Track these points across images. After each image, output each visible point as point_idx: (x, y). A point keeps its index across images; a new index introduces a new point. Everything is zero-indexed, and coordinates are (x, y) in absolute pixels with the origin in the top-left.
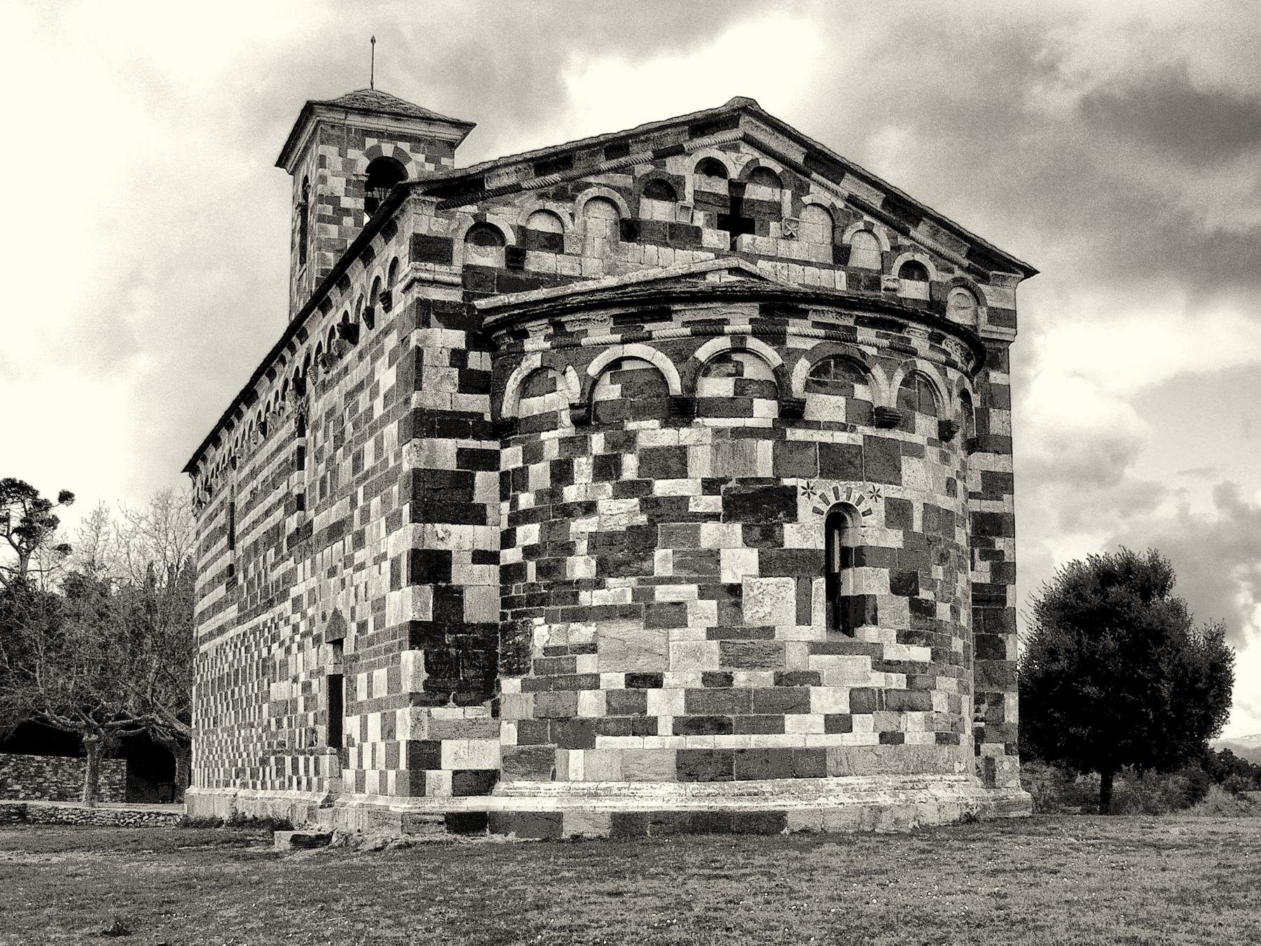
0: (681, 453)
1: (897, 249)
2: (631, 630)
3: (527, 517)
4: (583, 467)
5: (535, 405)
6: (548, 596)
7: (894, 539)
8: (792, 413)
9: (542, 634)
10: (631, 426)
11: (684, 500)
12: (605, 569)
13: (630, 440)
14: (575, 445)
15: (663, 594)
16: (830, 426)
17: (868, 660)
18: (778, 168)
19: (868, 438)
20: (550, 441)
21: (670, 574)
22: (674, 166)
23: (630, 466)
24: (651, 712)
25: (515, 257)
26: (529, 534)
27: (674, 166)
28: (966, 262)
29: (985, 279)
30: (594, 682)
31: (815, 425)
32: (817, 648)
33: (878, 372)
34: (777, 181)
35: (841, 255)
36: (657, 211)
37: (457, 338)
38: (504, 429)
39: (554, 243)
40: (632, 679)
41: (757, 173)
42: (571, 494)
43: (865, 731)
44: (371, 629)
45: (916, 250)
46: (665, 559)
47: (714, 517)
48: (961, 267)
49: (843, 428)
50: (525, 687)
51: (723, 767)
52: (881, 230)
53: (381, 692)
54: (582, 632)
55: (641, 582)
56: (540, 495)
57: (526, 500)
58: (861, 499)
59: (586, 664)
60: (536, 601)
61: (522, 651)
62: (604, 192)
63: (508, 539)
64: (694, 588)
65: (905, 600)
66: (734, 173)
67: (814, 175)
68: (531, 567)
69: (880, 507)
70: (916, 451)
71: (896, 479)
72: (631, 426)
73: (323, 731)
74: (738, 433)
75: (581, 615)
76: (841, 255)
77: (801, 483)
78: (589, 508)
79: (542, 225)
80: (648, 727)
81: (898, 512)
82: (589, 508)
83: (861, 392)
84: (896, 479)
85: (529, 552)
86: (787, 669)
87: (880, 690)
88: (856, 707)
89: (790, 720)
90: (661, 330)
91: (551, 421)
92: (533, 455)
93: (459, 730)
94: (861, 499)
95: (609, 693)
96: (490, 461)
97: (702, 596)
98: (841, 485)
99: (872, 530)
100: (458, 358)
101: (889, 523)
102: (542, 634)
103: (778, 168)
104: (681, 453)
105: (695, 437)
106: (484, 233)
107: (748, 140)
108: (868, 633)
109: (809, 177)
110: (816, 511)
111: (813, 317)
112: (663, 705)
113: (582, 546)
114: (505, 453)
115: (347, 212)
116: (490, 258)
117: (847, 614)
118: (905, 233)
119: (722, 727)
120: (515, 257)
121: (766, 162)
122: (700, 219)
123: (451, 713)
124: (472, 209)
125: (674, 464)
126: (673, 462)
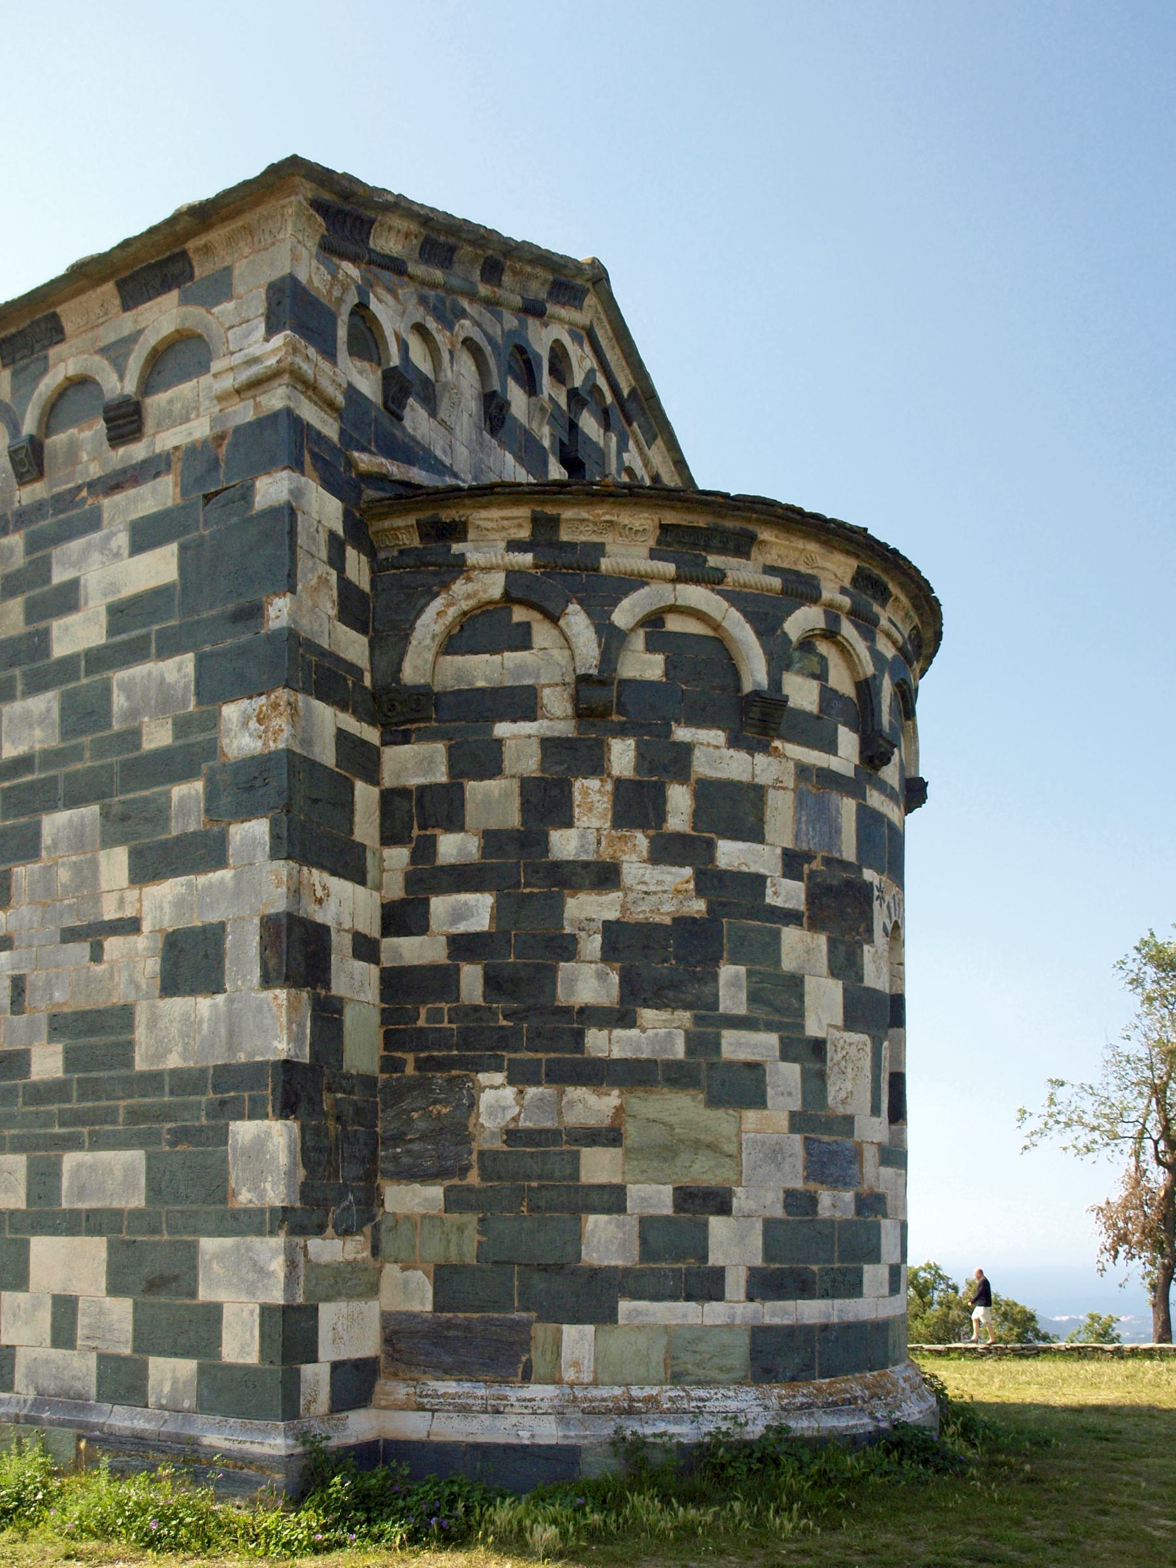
2: (682, 1108)
3: (463, 878)
4: (592, 797)
5: (483, 669)
6: (516, 1032)
10: (682, 734)
11: (758, 882)
13: (678, 761)
14: (574, 755)
15: (737, 1046)
21: (742, 1010)
23: (680, 802)
26: (477, 911)
30: (612, 1199)
40: (686, 1198)
42: (565, 844)
46: (734, 983)
47: (791, 917)
50: (454, 1201)
54: (592, 1105)
55: (698, 1020)
56: (492, 839)
57: (452, 847)
59: (598, 1166)
60: (480, 1044)
61: (458, 1132)
68: (471, 978)
72: (682, 734)
75: (597, 1074)
78: (605, 876)
80: (709, 1286)
85: (464, 946)
90: (743, 572)
91: (522, 702)
92: (485, 760)
95: (647, 1223)
97: (785, 1057)
102: (498, 1102)
104: (755, 793)
105: (772, 769)
112: (733, 1244)
113: (593, 945)
119: (804, 1288)
123: (328, 1249)
126: (732, 808)
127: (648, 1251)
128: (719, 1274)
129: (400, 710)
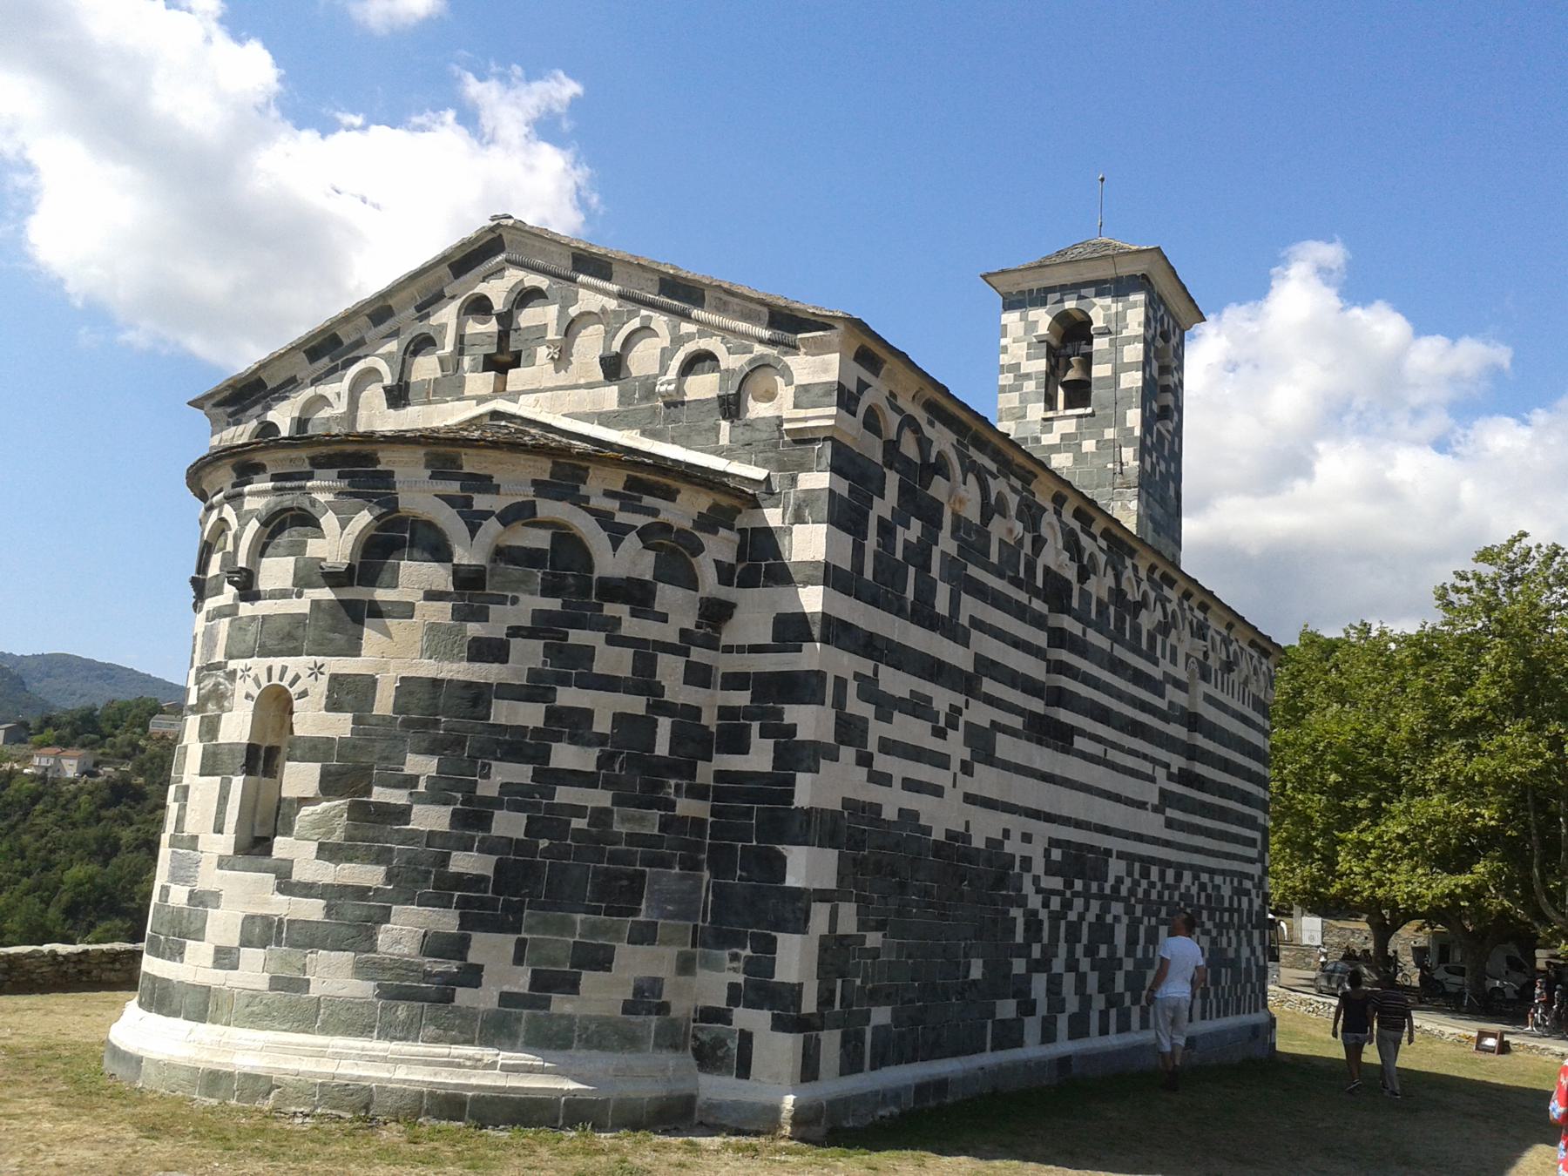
1: (678, 340)
7: (341, 725)
18: (542, 282)
19: (316, 604)
28: (767, 334)
32: (223, 863)
33: (329, 521)
35: (613, 367)
41: (527, 297)
43: (254, 970)
45: (701, 334)
48: (761, 341)
52: (660, 321)
58: (297, 678)
65: (341, 803)
66: (498, 305)
67: (582, 278)
71: (354, 650)
81: (349, 694)
84: (354, 650)
87: (281, 921)
94: (297, 678)
98: (277, 662)
101: (333, 706)
103: (542, 282)
109: (574, 280)
110: (248, 696)
111: (271, 470)
115: (1028, 376)
118: (687, 317)
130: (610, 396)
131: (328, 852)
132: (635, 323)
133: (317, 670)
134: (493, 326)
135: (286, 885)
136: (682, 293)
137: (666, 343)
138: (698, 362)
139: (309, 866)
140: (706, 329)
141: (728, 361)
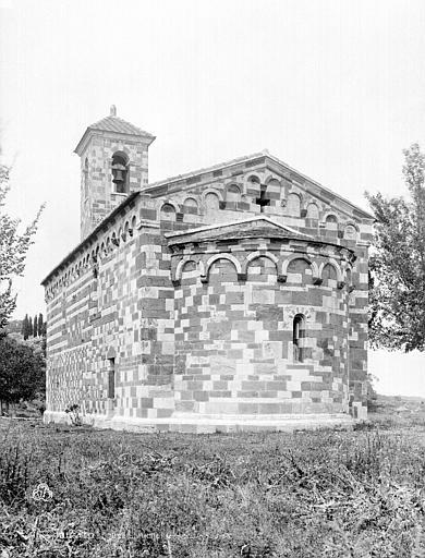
0: (242, 296)
2: (224, 360)
4: (205, 299)
5: (186, 275)
8: (282, 280)
9: (191, 360)
10: (223, 284)
11: (242, 312)
12: (214, 336)
15: (234, 346)
16: (295, 285)
17: (307, 371)
20: (194, 289)
21: (236, 339)
22: (239, 180)
23: (223, 299)
24: (229, 389)
25: (180, 217)
26: (185, 323)
27: (239, 180)
29: (360, 222)
31: (290, 284)
32: (289, 367)
33: (314, 264)
34: (280, 184)
35: (304, 214)
36: (234, 197)
37: (158, 249)
38: (177, 284)
39: (193, 211)
41: (272, 180)
42: (201, 309)
43: (307, 396)
44: (126, 356)
49: (301, 285)
50: (184, 379)
51: (253, 409)
52: (319, 202)
53: (130, 378)
54: (207, 360)
57: (184, 311)
58: (307, 312)
59: (206, 371)
60: (188, 347)
61: (183, 365)
62: (213, 191)
63: (178, 324)
64: (245, 345)
68: (186, 335)
69: (314, 315)
70: (328, 294)
73: (106, 392)
74: (261, 288)
75: (206, 354)
76: (304, 214)
77: (285, 306)
78: (207, 314)
79: (190, 204)
80: (228, 394)
81: (320, 316)
82: (207, 314)
83: (308, 271)
85: (186, 329)
86: (279, 374)
88: (303, 389)
89: (280, 393)
92: (187, 293)
93: (158, 394)
94: (307, 312)
96: (170, 295)
98: (300, 307)
99: (310, 324)
100: (159, 256)
103: (280, 179)
106: (168, 207)
107: (267, 168)
108: (306, 362)
112: (234, 386)
113: (205, 328)
114: (176, 292)
116: (172, 217)
117: (301, 354)
119: (255, 395)
120: (180, 217)
121: (275, 176)
122: (249, 200)
124: (164, 198)
125: (238, 298)
127: (215, 387)
128: (230, 393)
129: (177, 284)
130: (301, 223)
131: (323, 363)
132: (311, 201)
133: (312, 310)
134: (257, 187)
135: (312, 373)
136: (327, 196)
137: (321, 210)
138: (330, 218)
139: (318, 368)
140: (334, 208)
141: (340, 221)
